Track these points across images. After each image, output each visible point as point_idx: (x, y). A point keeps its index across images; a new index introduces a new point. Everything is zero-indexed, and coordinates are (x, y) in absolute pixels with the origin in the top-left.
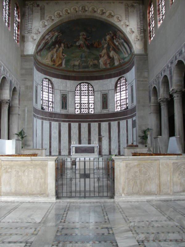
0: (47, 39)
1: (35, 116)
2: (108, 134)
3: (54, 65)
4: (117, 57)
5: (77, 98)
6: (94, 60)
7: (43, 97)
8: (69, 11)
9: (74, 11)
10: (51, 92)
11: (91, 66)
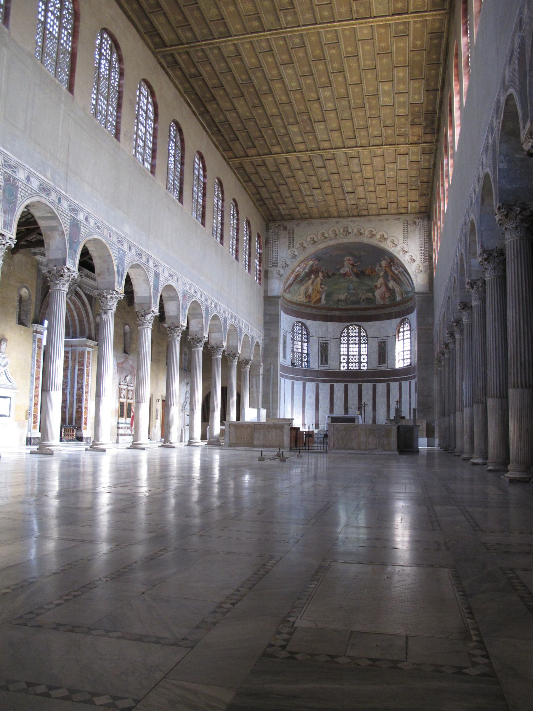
0: (298, 271)
1: (282, 376)
2: (386, 400)
3: (309, 302)
4: (398, 289)
5: (343, 349)
6: (368, 293)
7: (293, 348)
8: (326, 235)
9: (333, 235)
10: (306, 340)
11: (364, 300)
